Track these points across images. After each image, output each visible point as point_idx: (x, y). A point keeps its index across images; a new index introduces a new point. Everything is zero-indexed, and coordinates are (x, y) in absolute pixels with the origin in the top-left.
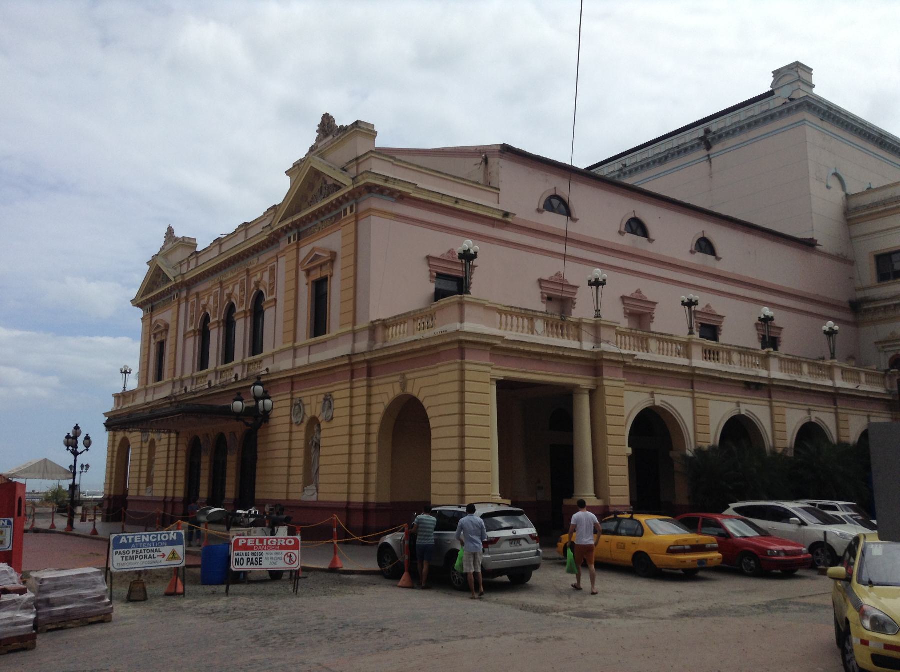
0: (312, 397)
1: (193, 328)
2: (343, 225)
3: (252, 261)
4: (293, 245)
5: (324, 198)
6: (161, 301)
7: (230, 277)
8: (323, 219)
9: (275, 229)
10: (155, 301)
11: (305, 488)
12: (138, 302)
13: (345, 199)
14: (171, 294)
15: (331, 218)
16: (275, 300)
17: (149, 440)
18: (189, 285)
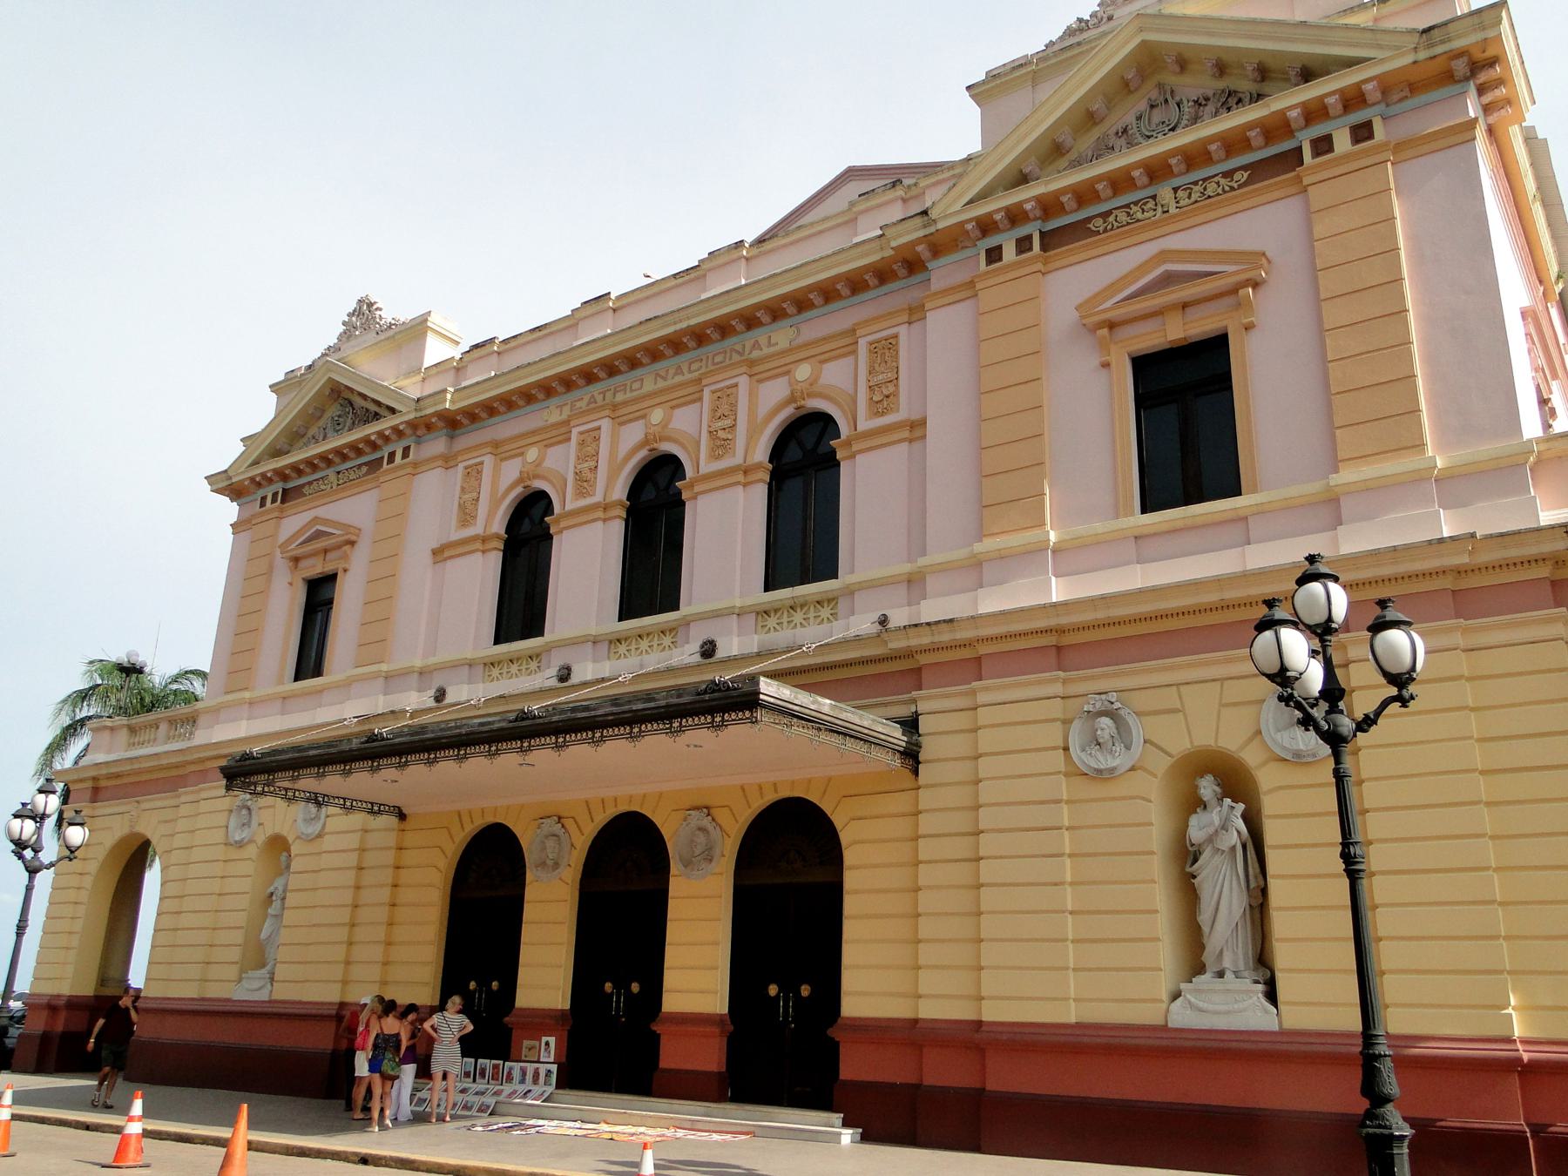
0: (1182, 688)
1: (477, 529)
2: (1305, 182)
3: (763, 340)
4: (1013, 266)
5: (1173, 129)
6: (330, 472)
7: (649, 386)
8: (1177, 182)
9: (940, 226)
10: (300, 473)
11: (1183, 986)
12: (234, 481)
13: (1353, 100)
14: (374, 447)
15: (1228, 174)
16: (916, 428)
17: (261, 839)
18: (453, 423)
